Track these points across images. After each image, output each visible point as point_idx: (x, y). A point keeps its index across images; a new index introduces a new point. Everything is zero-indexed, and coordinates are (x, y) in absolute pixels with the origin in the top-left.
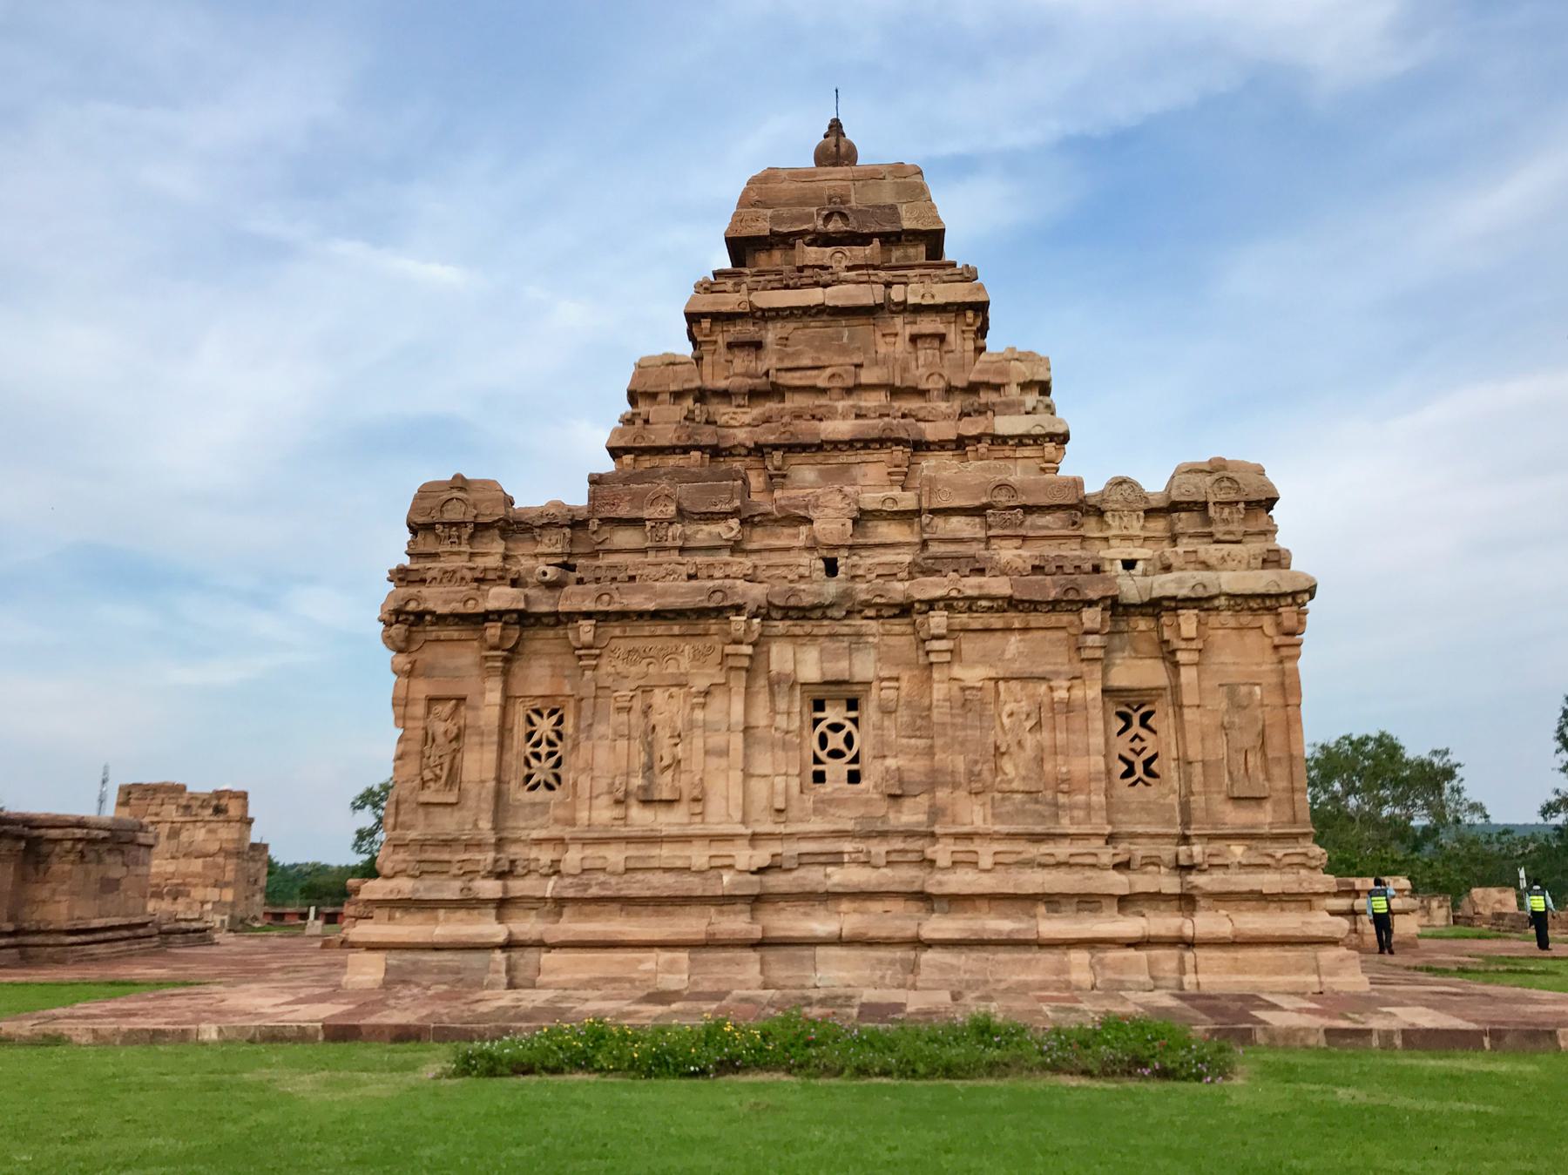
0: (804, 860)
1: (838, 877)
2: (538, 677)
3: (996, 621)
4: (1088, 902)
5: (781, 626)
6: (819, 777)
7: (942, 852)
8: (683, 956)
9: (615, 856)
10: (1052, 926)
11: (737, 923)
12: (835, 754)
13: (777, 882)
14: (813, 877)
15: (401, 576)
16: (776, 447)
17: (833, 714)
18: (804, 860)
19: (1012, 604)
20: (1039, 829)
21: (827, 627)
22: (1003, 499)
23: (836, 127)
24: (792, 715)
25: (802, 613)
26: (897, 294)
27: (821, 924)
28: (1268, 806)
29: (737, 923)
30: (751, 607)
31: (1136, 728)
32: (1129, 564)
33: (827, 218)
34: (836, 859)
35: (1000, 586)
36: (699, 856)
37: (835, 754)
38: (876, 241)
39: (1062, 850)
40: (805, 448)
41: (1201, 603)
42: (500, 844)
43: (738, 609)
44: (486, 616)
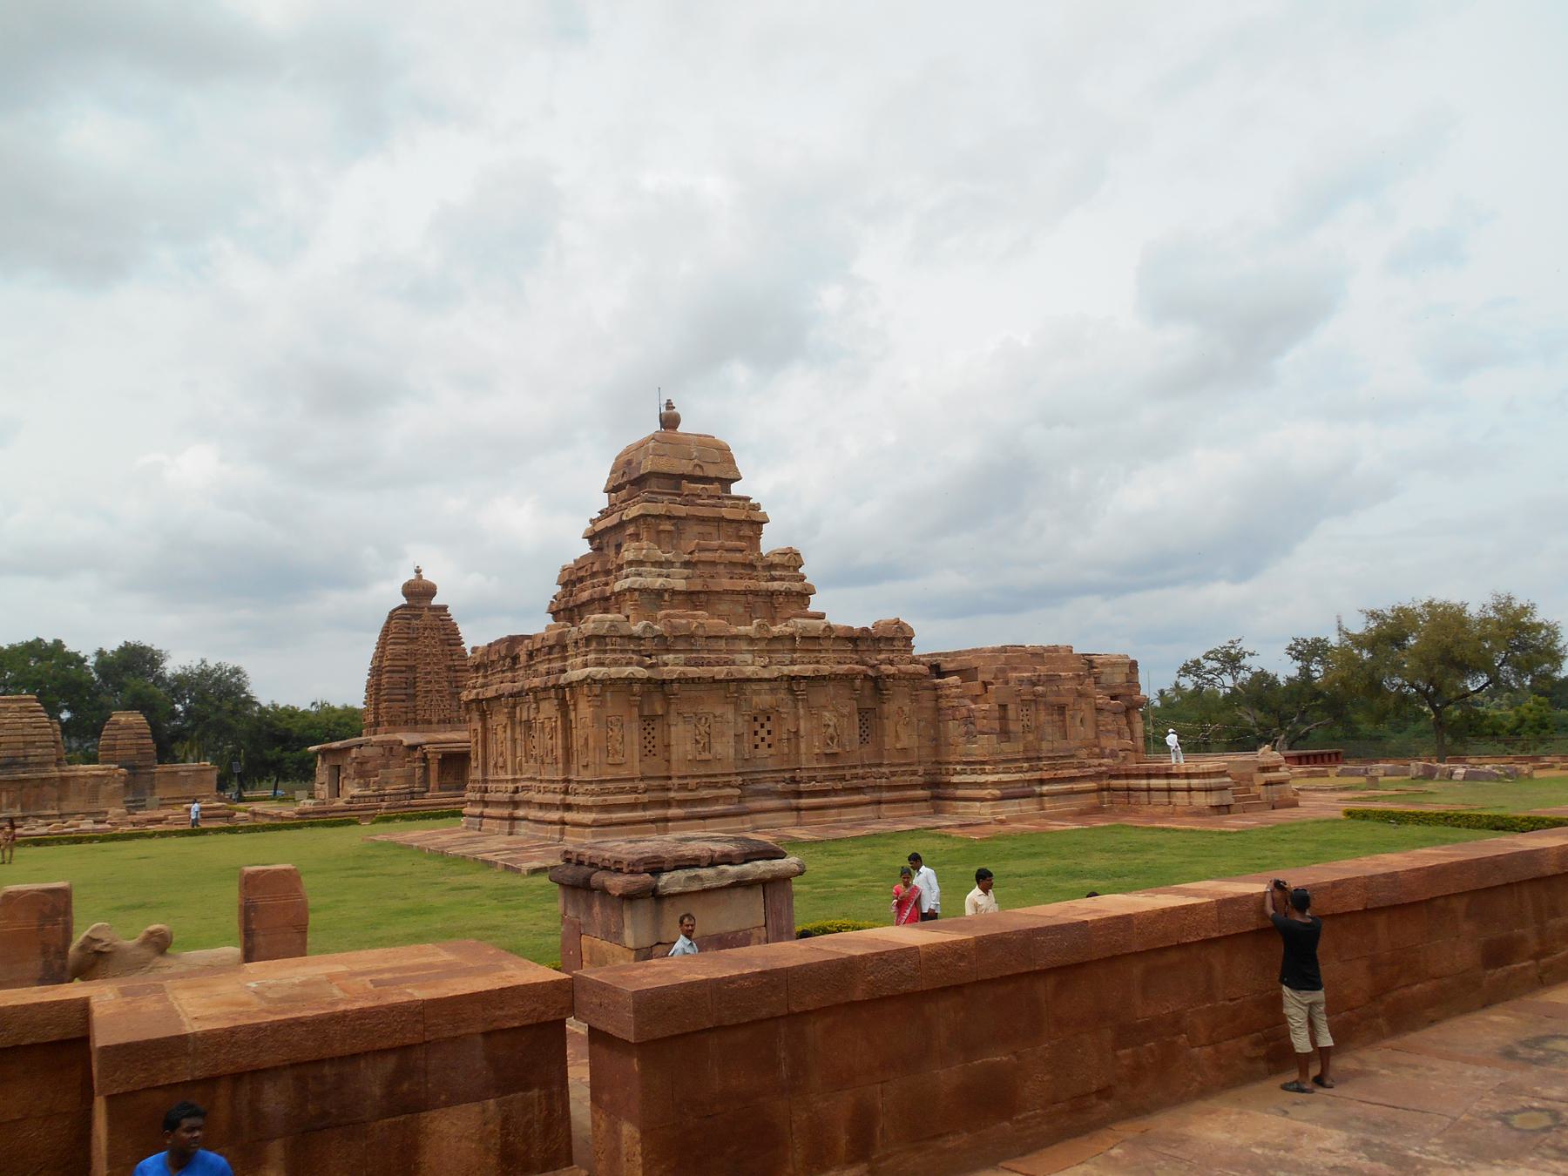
13: (518, 797)
23: (669, 405)
29: (506, 812)
41: (570, 684)
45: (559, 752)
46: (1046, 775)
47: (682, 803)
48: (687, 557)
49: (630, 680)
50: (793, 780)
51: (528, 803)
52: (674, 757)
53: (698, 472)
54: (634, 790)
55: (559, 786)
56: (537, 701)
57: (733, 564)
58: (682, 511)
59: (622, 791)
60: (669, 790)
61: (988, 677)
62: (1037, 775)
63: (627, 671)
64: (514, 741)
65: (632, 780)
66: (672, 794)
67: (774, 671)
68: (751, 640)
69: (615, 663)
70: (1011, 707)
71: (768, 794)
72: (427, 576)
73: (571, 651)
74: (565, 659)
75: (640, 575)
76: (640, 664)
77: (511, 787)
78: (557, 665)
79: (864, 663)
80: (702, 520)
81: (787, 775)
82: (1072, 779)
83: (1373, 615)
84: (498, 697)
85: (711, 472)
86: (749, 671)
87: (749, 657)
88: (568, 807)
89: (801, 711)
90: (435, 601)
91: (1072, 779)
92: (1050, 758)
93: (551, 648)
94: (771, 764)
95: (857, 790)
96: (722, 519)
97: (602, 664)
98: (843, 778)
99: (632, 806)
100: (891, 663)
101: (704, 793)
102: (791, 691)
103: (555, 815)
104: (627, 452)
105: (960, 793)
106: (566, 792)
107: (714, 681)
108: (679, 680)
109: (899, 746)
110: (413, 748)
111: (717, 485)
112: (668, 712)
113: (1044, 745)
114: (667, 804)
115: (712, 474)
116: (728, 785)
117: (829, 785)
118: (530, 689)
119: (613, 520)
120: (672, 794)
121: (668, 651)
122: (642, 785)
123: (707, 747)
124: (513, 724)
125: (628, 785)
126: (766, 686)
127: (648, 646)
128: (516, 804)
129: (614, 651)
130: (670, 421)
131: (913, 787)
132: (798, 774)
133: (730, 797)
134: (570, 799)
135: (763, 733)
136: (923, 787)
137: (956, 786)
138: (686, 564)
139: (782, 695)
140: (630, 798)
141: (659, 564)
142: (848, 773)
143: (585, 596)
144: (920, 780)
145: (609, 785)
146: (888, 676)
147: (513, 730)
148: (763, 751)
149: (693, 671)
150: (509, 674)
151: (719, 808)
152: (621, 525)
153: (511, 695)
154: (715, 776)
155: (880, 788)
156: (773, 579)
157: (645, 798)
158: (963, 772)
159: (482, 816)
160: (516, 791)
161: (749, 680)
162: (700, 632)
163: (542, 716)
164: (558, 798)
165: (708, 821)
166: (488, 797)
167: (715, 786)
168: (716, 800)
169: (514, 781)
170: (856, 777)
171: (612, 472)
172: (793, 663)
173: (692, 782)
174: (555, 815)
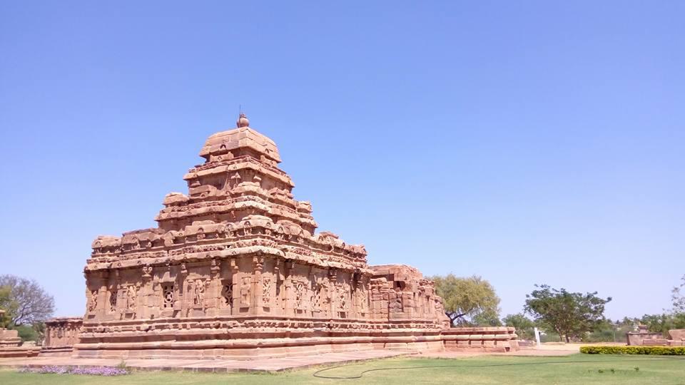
3: (197, 264)
4: (208, 337)
5: (157, 268)
6: (165, 306)
7: (180, 324)
8: (128, 351)
12: (169, 300)
14: (158, 332)
15: (89, 262)
16: (189, 217)
20: (200, 318)
22: (201, 231)
26: (231, 168)
28: (249, 310)
30: (148, 264)
31: (230, 290)
32: (228, 246)
33: (221, 147)
36: (134, 327)
37: (169, 300)
38: (229, 153)
39: (203, 323)
40: (195, 216)
41: (235, 257)
43: (145, 265)
46: (428, 330)
47: (293, 335)
48: (272, 196)
49: (277, 257)
50: (329, 326)
52: (288, 306)
53: (266, 153)
58: (264, 171)
59: (269, 325)
60: (286, 326)
62: (423, 330)
63: (275, 251)
65: (272, 318)
66: (288, 329)
67: (325, 264)
68: (315, 245)
75: (254, 200)
80: (271, 178)
81: (327, 323)
85: (271, 155)
86: (318, 262)
87: (314, 253)
92: (427, 322)
94: (320, 316)
95: (350, 334)
96: (279, 180)
97: (264, 245)
98: (345, 327)
100: (362, 267)
101: (300, 330)
107: (307, 263)
109: (362, 311)
113: (425, 315)
114: (283, 335)
115: (271, 156)
116: (309, 326)
118: (182, 261)
120: (288, 329)
121: (289, 243)
122: (278, 322)
126: (320, 271)
127: (279, 238)
128: (146, 339)
129: (269, 238)
132: (332, 323)
135: (317, 298)
138: (270, 200)
141: (260, 196)
142: (349, 324)
143: (202, 210)
144: (368, 331)
145: (263, 321)
146: (362, 274)
149: (302, 257)
151: (305, 339)
152: (224, 173)
153: (151, 265)
154: (303, 320)
155: (355, 334)
156: (302, 216)
157: (280, 330)
158: (393, 327)
162: (301, 235)
167: (302, 326)
170: (351, 327)
172: (330, 260)
173: (296, 323)
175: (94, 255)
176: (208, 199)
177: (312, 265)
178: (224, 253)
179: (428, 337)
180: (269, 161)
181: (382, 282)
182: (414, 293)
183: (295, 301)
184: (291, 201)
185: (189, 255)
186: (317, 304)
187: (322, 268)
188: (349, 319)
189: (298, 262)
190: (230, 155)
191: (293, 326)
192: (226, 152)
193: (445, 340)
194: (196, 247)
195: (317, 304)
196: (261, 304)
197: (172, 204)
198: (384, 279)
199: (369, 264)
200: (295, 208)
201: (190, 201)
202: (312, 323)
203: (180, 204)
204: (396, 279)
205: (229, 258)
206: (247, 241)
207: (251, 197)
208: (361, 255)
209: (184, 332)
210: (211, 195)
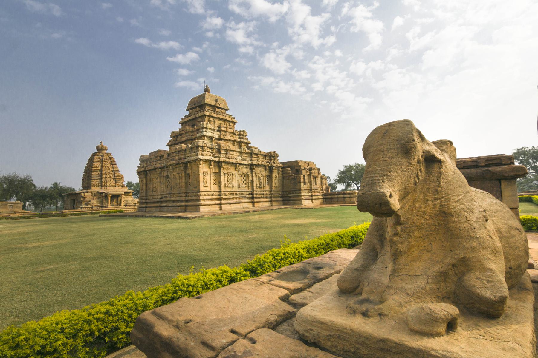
0: (165, 197)
1: (168, 199)
2: (148, 177)
4: (182, 201)
9: (151, 197)
10: (178, 204)
11: (158, 205)
13: (162, 200)
14: (165, 199)
17: (168, 179)
18: (165, 197)
19: (176, 164)
21: (165, 169)
24: (163, 180)
25: (163, 167)
26: (197, 116)
27: (164, 205)
29: (158, 205)
34: (167, 197)
35: (174, 162)
36: (156, 197)
41: (190, 162)
42: (146, 196)
44: (142, 171)
45: (184, 184)
49: (210, 161)
50: (251, 194)
51: (166, 201)
53: (218, 106)
54: (212, 195)
55: (184, 195)
56: (173, 169)
57: (230, 132)
58: (215, 115)
59: (208, 195)
61: (297, 168)
62: (310, 194)
64: (161, 182)
69: (207, 155)
70: (306, 176)
71: (245, 197)
72: (103, 144)
73: (188, 151)
74: (185, 154)
76: (213, 156)
77: (159, 197)
78: (183, 156)
79: (267, 162)
80: (221, 119)
82: (318, 195)
83: (346, 167)
84: (155, 169)
85: (221, 106)
88: (186, 201)
89: (254, 175)
90: (107, 152)
91: (318, 195)
93: (179, 151)
99: (211, 200)
100: (274, 163)
102: (251, 169)
103: (183, 204)
104: (195, 98)
105: (292, 199)
106: (186, 196)
107: (233, 163)
108: (224, 162)
110: (102, 193)
111: (223, 111)
112: (220, 172)
116: (236, 195)
117: (260, 196)
118: (170, 165)
119: (193, 117)
123: (230, 183)
124: (160, 177)
125: (210, 193)
126: (245, 167)
128: (161, 202)
130: (207, 90)
131: (278, 197)
133: (236, 198)
134: (187, 198)
135: (244, 180)
136: (281, 197)
137: (290, 197)
138: (218, 131)
139: (249, 170)
140: (210, 197)
142: (265, 192)
143: (184, 139)
147: (160, 179)
148: (244, 185)
149: (227, 160)
150: (159, 162)
151: (234, 201)
152: (196, 118)
153: (160, 168)
158: (293, 193)
159: (146, 207)
160: (162, 198)
161: (240, 164)
163: (175, 173)
164: (183, 198)
165: (232, 205)
166: (148, 201)
167: (233, 195)
168: (233, 198)
169: (161, 195)
171: (189, 104)
173: (227, 193)
174: (183, 204)
175: (140, 164)
176: (187, 132)
177: (236, 164)
178: (186, 160)
179: (314, 197)
180: (217, 110)
181: (287, 170)
182: (304, 176)
183: (226, 183)
184: (232, 131)
185: (172, 162)
186: (244, 184)
187: (245, 165)
188: (265, 189)
189: (226, 163)
190: (198, 109)
191: (225, 195)
192: (196, 108)
193: (325, 198)
194: (175, 158)
195: (244, 184)
196: (201, 184)
197: (174, 137)
198: (289, 169)
199: (280, 161)
200: (235, 134)
201: (180, 135)
202: (238, 193)
203: (177, 136)
204: (296, 168)
205: (186, 163)
206: (194, 154)
207: (205, 130)
208: (274, 157)
209: (173, 199)
210: (188, 131)
